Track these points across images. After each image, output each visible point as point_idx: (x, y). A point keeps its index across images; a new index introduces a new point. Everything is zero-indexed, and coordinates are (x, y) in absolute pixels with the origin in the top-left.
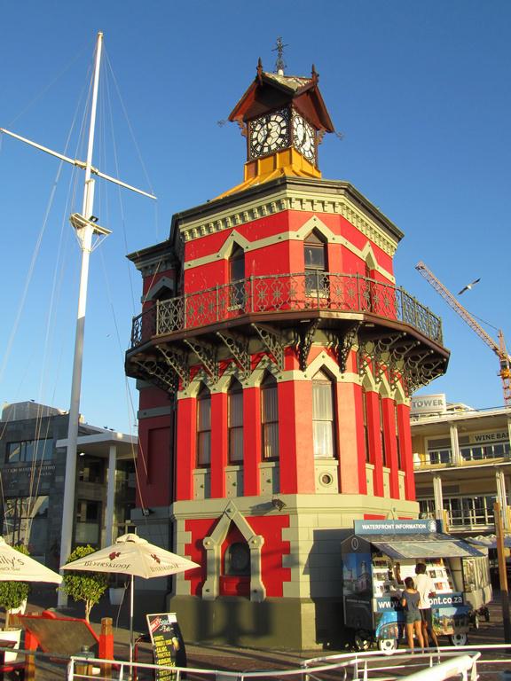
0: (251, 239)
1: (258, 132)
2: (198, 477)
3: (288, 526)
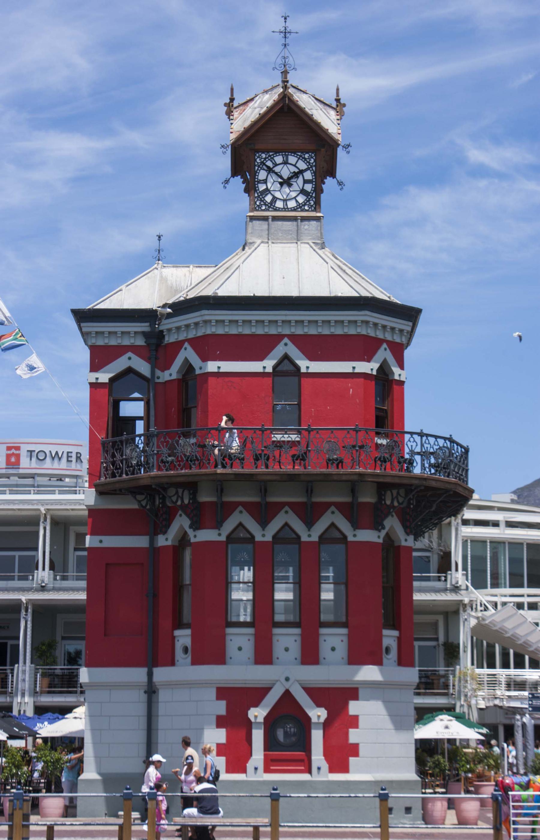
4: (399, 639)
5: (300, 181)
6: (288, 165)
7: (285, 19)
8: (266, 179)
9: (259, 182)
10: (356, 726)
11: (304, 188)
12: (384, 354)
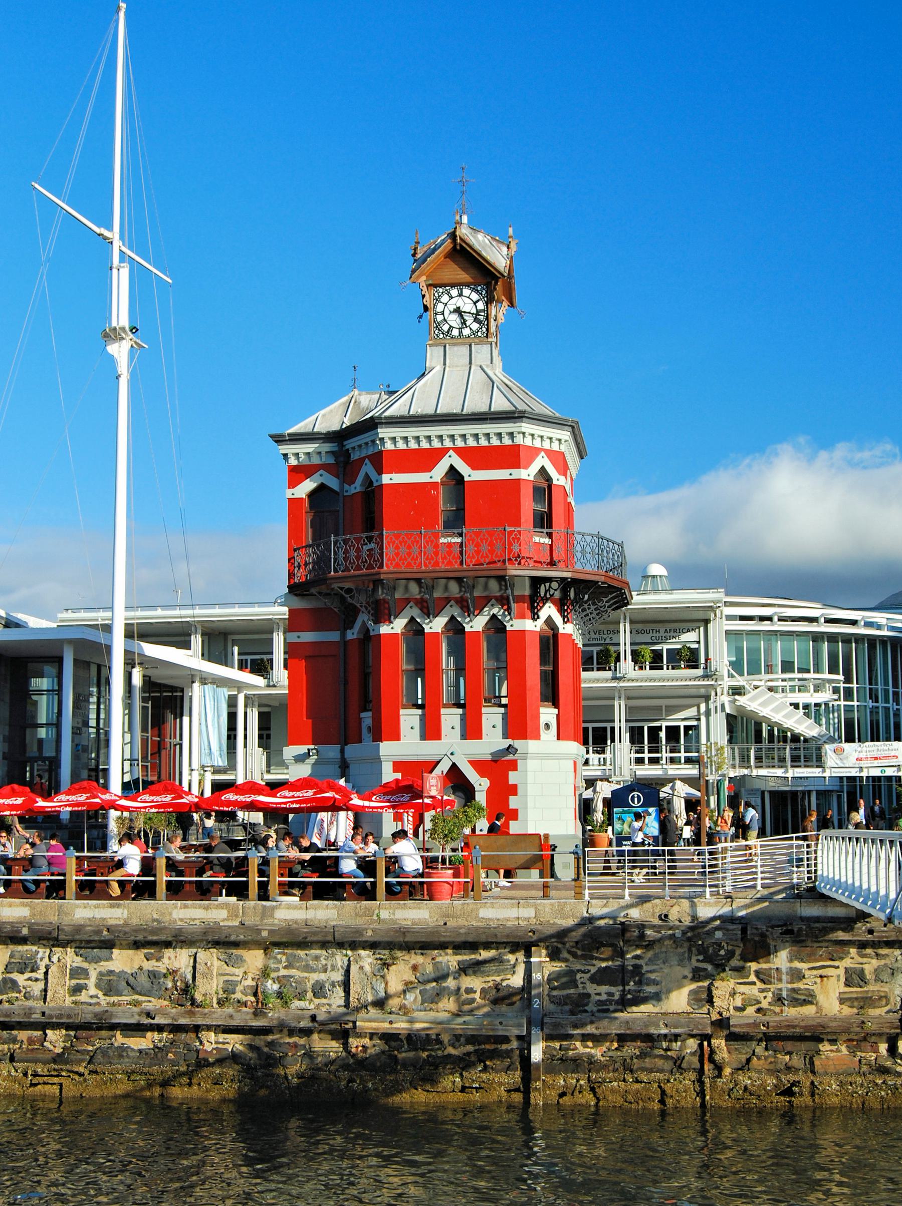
0: (475, 466)
2: (410, 719)
3: (516, 770)
4: (558, 716)
10: (515, 794)
12: (542, 461)
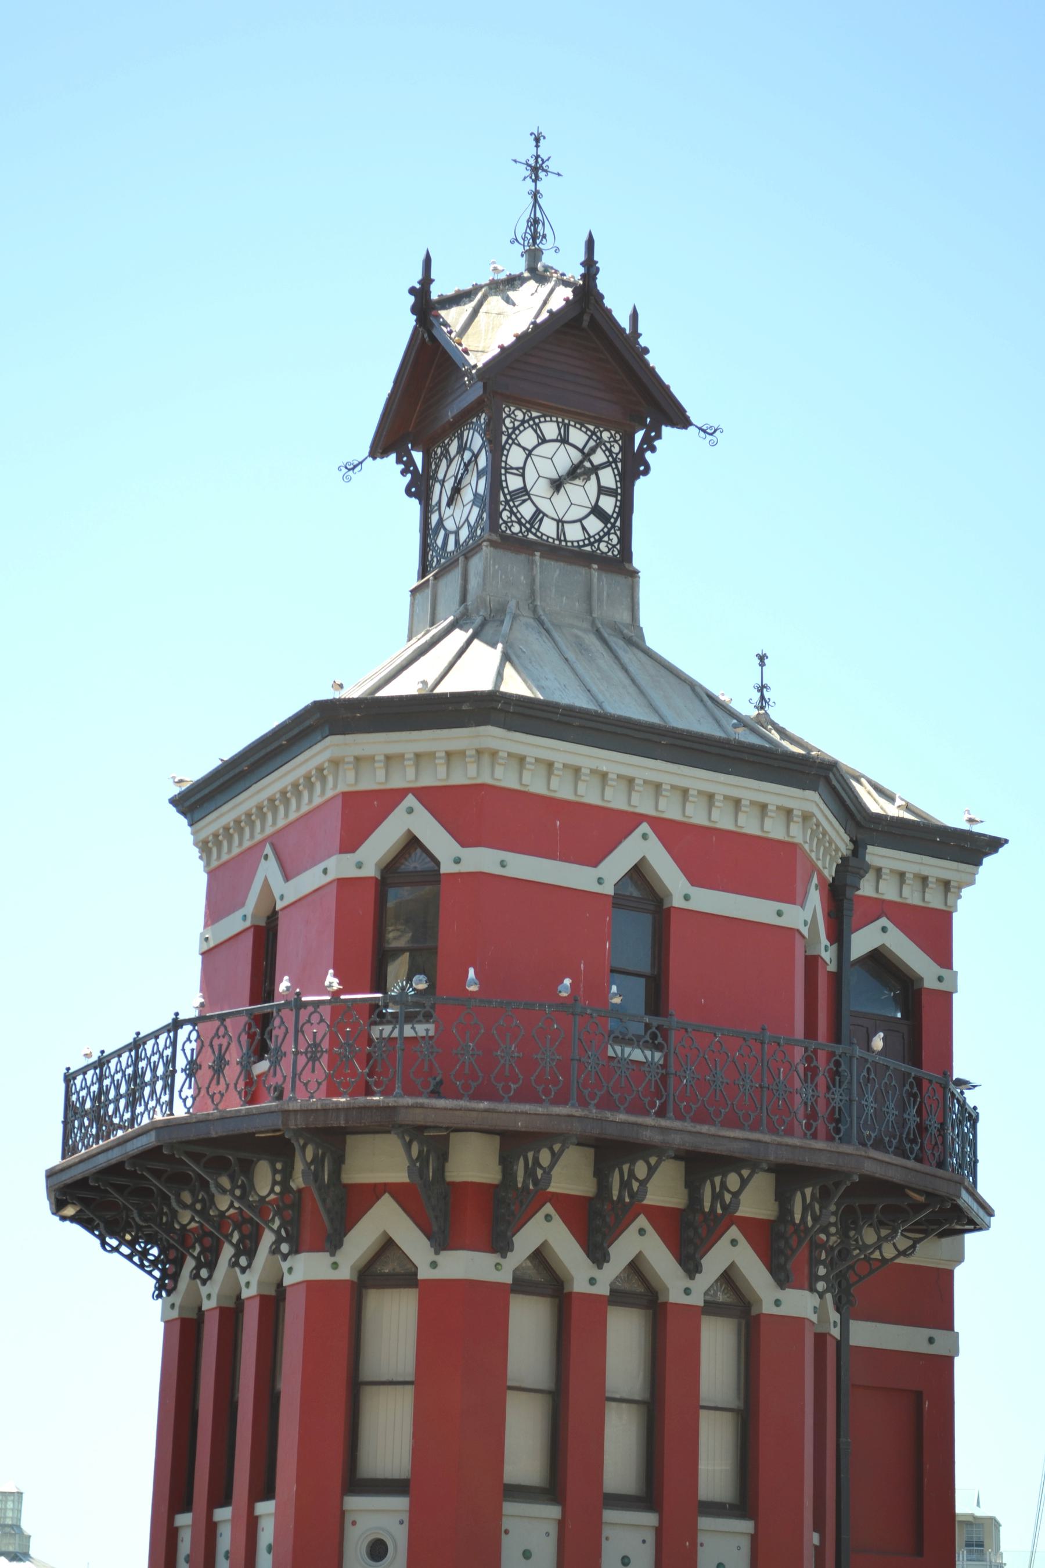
1: (529, 453)
5: (592, 486)
6: (567, 446)
7: (537, 140)
8: (524, 468)
9: (508, 469)
11: (600, 504)
